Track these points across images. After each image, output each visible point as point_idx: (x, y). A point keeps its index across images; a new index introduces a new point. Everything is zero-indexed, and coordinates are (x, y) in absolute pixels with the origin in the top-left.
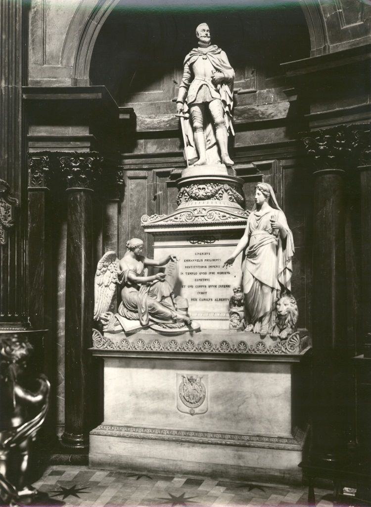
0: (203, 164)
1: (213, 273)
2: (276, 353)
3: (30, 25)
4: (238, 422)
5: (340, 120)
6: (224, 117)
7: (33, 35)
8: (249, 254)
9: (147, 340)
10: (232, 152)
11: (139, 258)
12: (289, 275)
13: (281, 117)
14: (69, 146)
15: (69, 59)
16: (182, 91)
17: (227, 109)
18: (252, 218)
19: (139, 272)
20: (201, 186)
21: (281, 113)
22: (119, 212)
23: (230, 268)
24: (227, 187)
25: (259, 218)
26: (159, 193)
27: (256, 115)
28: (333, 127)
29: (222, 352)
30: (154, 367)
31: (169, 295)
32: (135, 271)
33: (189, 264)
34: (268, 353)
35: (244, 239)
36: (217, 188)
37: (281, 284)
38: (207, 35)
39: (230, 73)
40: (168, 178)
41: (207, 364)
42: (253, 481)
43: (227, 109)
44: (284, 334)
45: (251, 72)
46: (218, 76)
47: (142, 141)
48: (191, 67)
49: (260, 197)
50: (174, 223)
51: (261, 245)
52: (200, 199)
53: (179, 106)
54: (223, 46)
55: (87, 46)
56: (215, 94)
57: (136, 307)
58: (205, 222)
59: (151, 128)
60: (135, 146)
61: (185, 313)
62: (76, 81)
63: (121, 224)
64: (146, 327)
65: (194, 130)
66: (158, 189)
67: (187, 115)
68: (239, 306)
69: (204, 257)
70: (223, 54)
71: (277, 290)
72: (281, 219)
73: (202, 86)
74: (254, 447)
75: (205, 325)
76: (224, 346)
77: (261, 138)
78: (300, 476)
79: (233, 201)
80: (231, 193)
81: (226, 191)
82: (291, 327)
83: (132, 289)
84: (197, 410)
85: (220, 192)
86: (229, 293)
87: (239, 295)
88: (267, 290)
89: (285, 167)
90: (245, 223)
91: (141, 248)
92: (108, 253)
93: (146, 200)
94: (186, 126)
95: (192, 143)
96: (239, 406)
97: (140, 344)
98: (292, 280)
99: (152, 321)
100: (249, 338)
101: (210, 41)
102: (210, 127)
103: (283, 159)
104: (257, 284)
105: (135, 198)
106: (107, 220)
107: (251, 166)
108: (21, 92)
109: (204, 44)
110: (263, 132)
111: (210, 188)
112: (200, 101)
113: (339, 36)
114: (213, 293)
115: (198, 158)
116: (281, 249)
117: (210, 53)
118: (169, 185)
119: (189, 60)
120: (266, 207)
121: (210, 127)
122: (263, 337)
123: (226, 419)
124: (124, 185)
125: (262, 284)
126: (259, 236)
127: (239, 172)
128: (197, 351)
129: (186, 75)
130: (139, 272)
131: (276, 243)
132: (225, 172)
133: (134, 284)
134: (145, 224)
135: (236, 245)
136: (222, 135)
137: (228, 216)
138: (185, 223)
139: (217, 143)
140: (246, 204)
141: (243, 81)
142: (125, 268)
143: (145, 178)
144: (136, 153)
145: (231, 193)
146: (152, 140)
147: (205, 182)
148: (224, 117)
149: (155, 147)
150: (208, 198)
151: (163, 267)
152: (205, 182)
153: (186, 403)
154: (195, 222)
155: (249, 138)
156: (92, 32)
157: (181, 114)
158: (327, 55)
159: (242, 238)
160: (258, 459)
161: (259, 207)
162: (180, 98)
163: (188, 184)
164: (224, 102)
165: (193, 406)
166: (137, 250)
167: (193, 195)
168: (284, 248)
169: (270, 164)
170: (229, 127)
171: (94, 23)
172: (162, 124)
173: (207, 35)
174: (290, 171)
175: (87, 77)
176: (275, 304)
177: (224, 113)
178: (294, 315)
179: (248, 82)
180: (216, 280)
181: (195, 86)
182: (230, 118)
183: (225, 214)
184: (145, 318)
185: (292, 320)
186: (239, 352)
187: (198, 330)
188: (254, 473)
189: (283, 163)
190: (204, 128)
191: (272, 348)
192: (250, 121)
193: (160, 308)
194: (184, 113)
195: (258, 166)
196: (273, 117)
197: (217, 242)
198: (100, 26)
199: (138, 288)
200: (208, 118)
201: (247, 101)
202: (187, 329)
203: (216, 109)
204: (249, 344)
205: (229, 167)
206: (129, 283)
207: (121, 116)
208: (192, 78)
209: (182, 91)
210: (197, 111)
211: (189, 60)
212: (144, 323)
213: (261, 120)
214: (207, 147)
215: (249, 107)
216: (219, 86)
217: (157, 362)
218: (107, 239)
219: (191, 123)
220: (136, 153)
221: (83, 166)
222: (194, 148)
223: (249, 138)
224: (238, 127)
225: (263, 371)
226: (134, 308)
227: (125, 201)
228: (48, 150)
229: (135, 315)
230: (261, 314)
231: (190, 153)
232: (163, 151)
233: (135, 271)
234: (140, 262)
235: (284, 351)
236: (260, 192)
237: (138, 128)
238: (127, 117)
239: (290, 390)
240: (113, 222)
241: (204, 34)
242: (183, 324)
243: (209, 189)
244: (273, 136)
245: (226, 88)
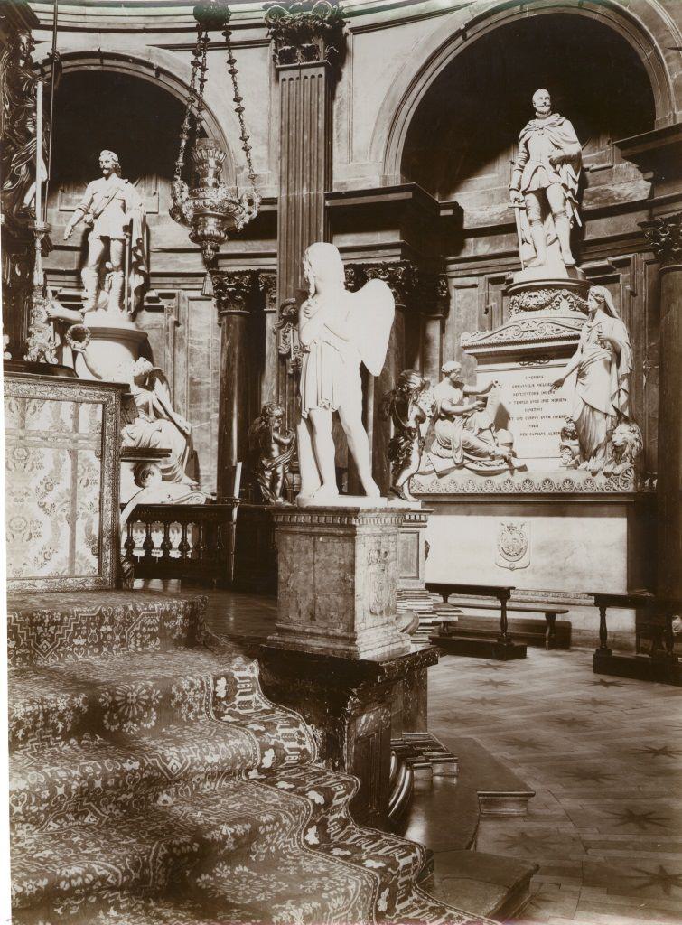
1: (547, 401)
2: (607, 491)
3: (334, 118)
4: (565, 577)
6: (565, 204)
7: (338, 129)
9: (463, 481)
11: (457, 385)
12: (624, 398)
13: (642, 198)
14: (377, 255)
15: (377, 153)
16: (517, 175)
17: (569, 194)
19: (455, 402)
20: (533, 294)
21: (641, 192)
22: (443, 331)
23: (559, 393)
24: (565, 292)
26: (492, 304)
28: (676, 214)
29: (544, 491)
30: (469, 514)
31: (488, 427)
33: (517, 390)
34: (598, 491)
36: (553, 295)
37: (616, 409)
38: (545, 103)
39: (573, 148)
40: (503, 285)
41: (530, 508)
42: (579, 646)
43: (569, 194)
44: (619, 469)
45: (606, 142)
46: (557, 154)
47: (471, 241)
50: (499, 341)
52: (531, 310)
53: (514, 194)
55: (398, 136)
57: (449, 444)
58: (535, 337)
59: (481, 224)
60: (462, 246)
61: (508, 449)
62: (385, 179)
63: (445, 346)
64: (461, 466)
66: (490, 299)
67: (523, 205)
68: (573, 438)
69: (536, 381)
71: (612, 416)
72: (617, 330)
73: (537, 168)
74: (580, 605)
76: (547, 485)
77: (618, 228)
78: (633, 640)
79: (575, 310)
80: (572, 300)
81: (565, 297)
82: (631, 462)
83: (447, 422)
84: (517, 565)
85: (557, 299)
86: (563, 424)
87: (571, 427)
88: (598, 416)
89: (648, 263)
90: (578, 337)
91: (458, 373)
93: (477, 314)
95: (529, 240)
96: (566, 559)
97: (452, 486)
98: (629, 402)
99: (468, 458)
100: (579, 478)
101: (551, 109)
103: (646, 251)
104: (587, 410)
105: (463, 311)
106: (427, 341)
107: (605, 263)
108: (323, 199)
109: (542, 115)
111: (544, 295)
112: (534, 187)
116: (614, 366)
117: (548, 127)
118: (505, 293)
119: (523, 137)
121: (550, 217)
122: (594, 474)
123: (550, 574)
124: (448, 297)
125: (593, 409)
128: (516, 492)
130: (455, 402)
131: (609, 358)
133: (449, 416)
134: (466, 344)
135: (565, 365)
136: (563, 228)
137: (562, 328)
138: (512, 340)
141: (597, 154)
143: (475, 286)
144: (464, 255)
145: (572, 300)
146: (484, 238)
147: (542, 287)
148: (565, 204)
149: (488, 246)
150: (542, 307)
151: (485, 395)
152: (542, 287)
153: (506, 556)
154: (524, 339)
155: (600, 229)
156: (404, 118)
157: (516, 204)
158: (669, 128)
159: (574, 356)
160: (585, 619)
162: (514, 185)
163: (517, 292)
164: (564, 186)
165: (511, 559)
166: (453, 375)
167: (523, 305)
168: (618, 366)
169: (629, 260)
170: (574, 216)
171: (406, 107)
172: (495, 217)
173: (545, 103)
175: (398, 173)
176: (610, 434)
177: (566, 199)
178: (633, 446)
181: (530, 167)
182: (574, 205)
183: (561, 328)
184: (459, 454)
185: (630, 453)
186: (564, 491)
188: (579, 637)
189: (646, 256)
190: (543, 219)
191: (603, 485)
192: (604, 206)
193: (475, 442)
194: (519, 202)
195: (614, 263)
196: (631, 198)
197: (552, 362)
198: (413, 111)
199: (453, 421)
200: (546, 209)
201: (602, 180)
202: (505, 466)
203: (556, 198)
204: (576, 482)
206: (443, 415)
207: (443, 213)
210: (533, 201)
211: (523, 137)
212: (458, 461)
213: (617, 204)
214: (548, 242)
215: (602, 187)
216: (558, 166)
217: (473, 507)
220: (464, 255)
222: (532, 246)
223: (600, 229)
224: (587, 216)
225: (594, 515)
226: (447, 445)
227: (450, 317)
228: (353, 262)
229: (448, 453)
230: (595, 447)
231: (525, 252)
232: (497, 251)
233: (451, 401)
234: (458, 390)
235: (616, 488)
236: (592, 298)
237: (466, 225)
238: (450, 212)
239: (626, 537)
240: (434, 344)
241: (541, 103)
242: (503, 460)
243: (543, 296)
244: (630, 223)
245: (568, 168)
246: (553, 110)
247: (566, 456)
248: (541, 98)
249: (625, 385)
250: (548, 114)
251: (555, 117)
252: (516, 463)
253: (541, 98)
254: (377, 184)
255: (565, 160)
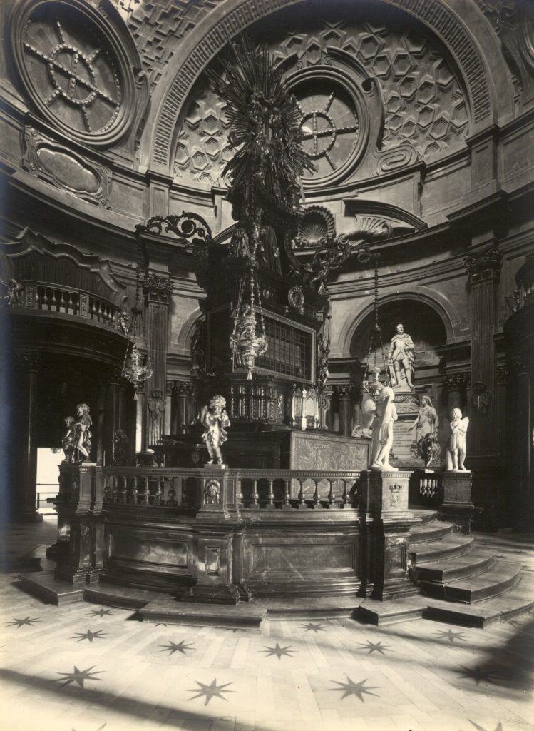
0: (400, 386)
5: (459, 369)
8: (419, 426)
10: (414, 380)
16: (390, 354)
18: (420, 411)
25: (424, 410)
27: (425, 364)
32: (369, 434)
35: (417, 420)
39: (412, 346)
46: (407, 348)
48: (394, 343)
49: (424, 402)
51: (424, 422)
54: (409, 333)
56: (405, 356)
62: (344, 355)
65: (396, 371)
69: (400, 428)
70: (409, 337)
72: (433, 411)
75: (400, 457)
86: (411, 443)
87: (415, 444)
92: (357, 427)
94: (391, 369)
102: (403, 370)
106: (355, 412)
107: (422, 386)
110: (427, 371)
112: (398, 359)
113: (458, 334)
114: (403, 443)
115: (398, 383)
120: (427, 406)
121: (403, 370)
126: (424, 418)
127: (416, 389)
129: (392, 347)
132: (410, 391)
136: (409, 374)
139: (406, 377)
140: (419, 404)
142: (365, 433)
147: (400, 395)
152: (400, 395)
155: (420, 374)
161: (424, 406)
174: (440, 388)
179: (422, 347)
180: (405, 438)
181: (396, 352)
187: (397, 458)
189: (438, 384)
190: (400, 370)
200: (402, 366)
203: (406, 362)
205: (411, 388)
208: (395, 348)
209: (390, 354)
210: (397, 363)
218: (355, 420)
219: (394, 368)
221: (347, 390)
223: (420, 374)
224: (416, 369)
233: (369, 434)
243: (402, 398)
245: (410, 353)
246: (404, 332)
247: (413, 455)
248: (400, 327)
249: (436, 430)
250: (402, 333)
251: (405, 335)
252: (395, 456)
253: (400, 327)
254: (341, 357)
255: (409, 350)
